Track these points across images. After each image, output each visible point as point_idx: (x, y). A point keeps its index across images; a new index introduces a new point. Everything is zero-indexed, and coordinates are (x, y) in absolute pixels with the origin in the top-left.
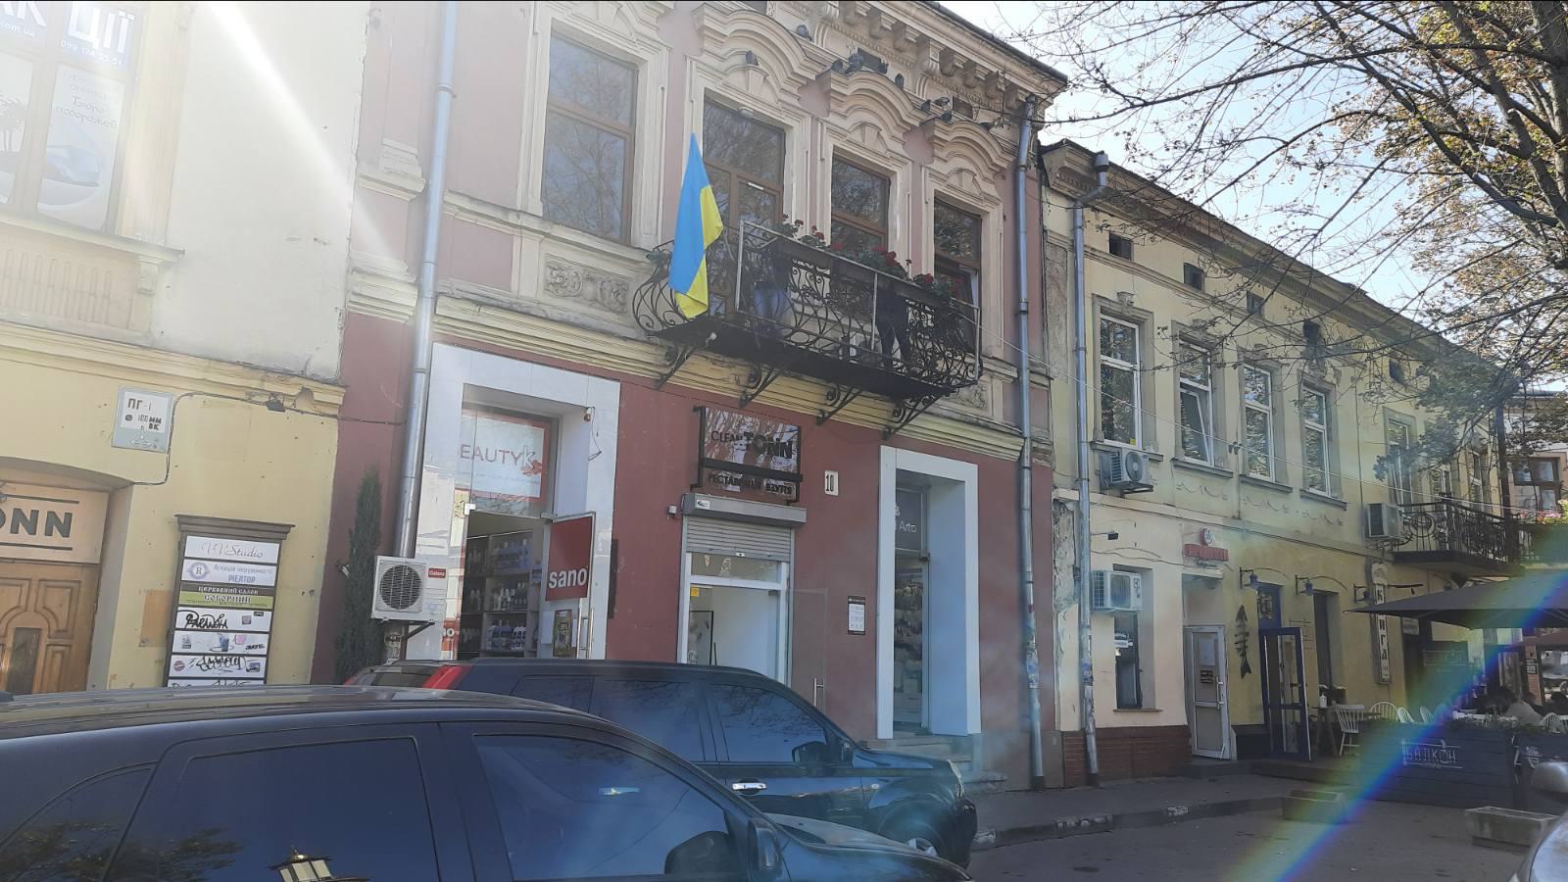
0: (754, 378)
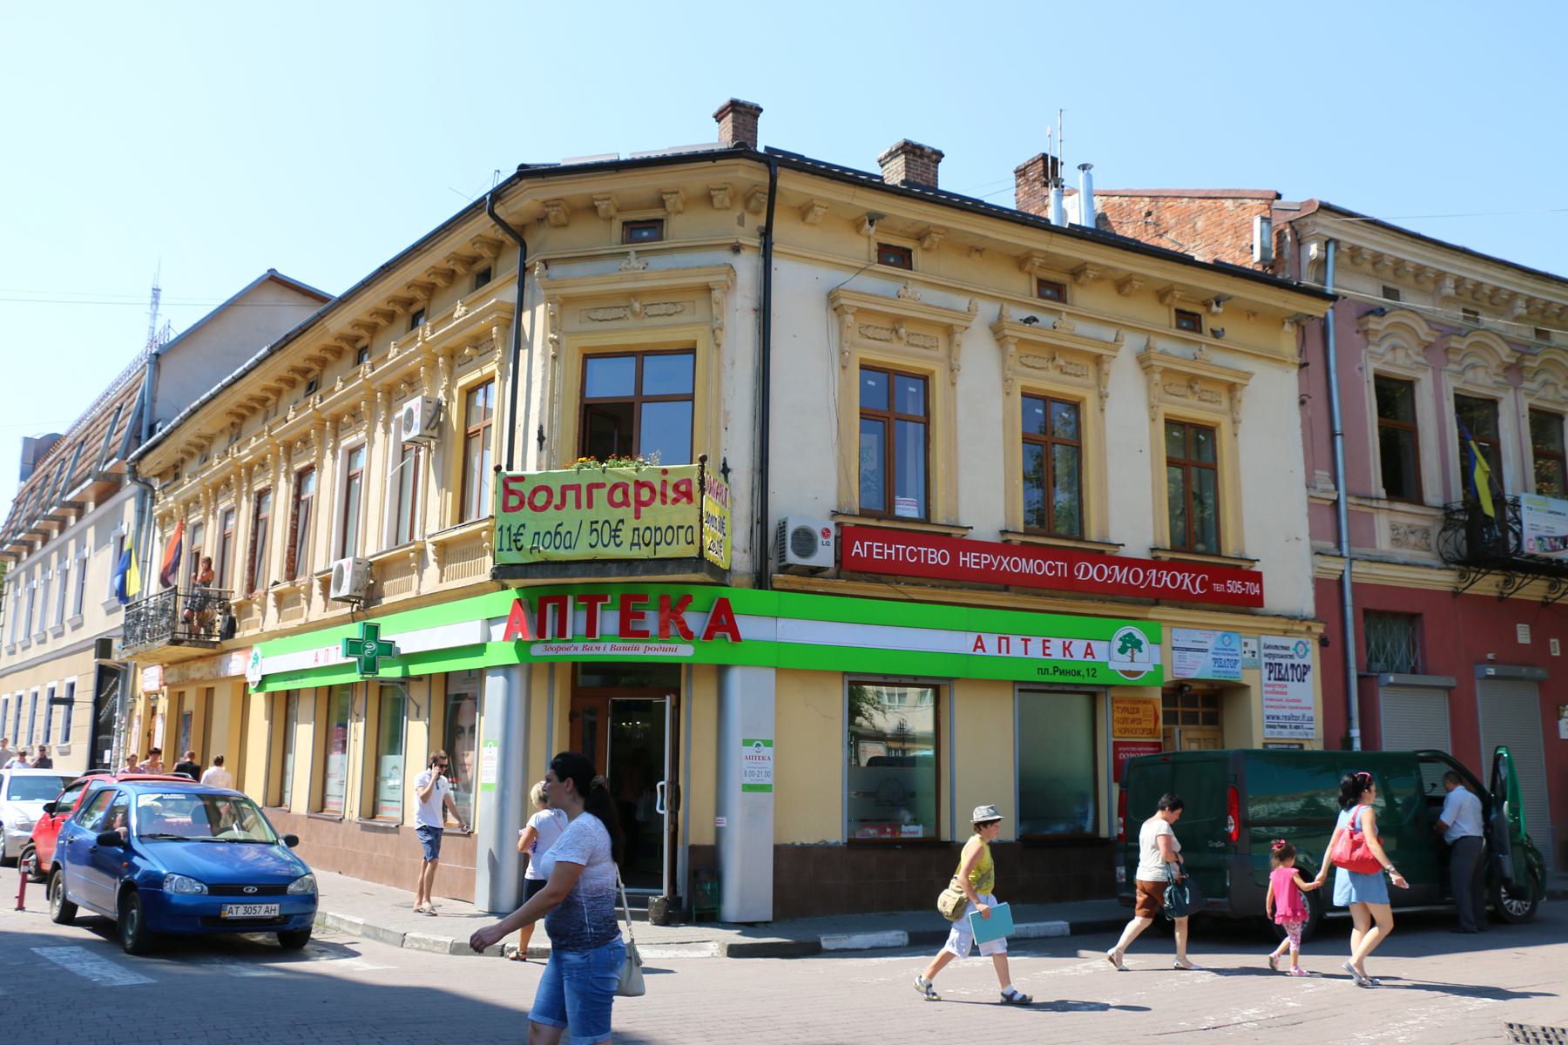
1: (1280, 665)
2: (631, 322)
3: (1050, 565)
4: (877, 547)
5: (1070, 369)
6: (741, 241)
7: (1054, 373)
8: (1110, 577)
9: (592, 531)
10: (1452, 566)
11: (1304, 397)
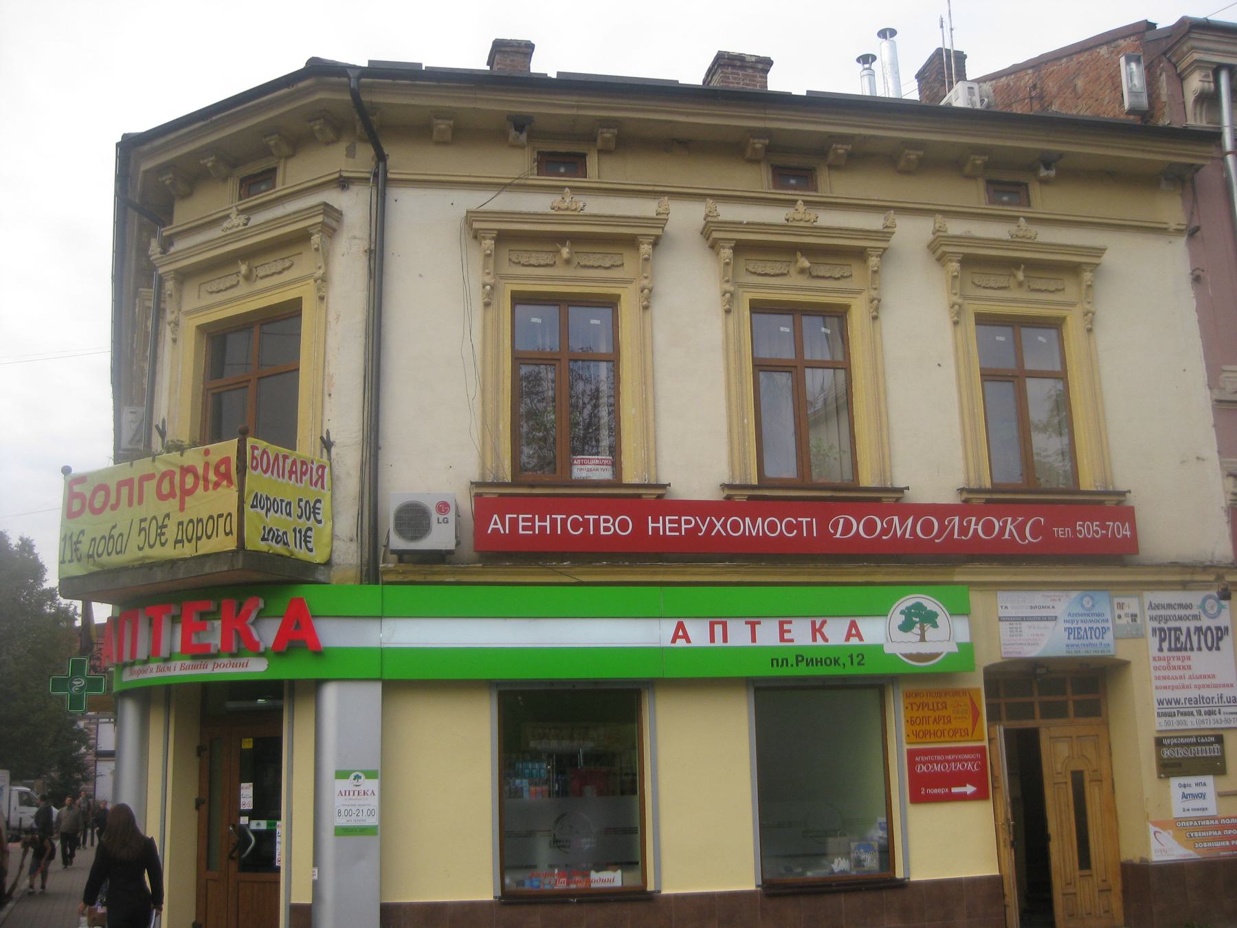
1: (1179, 629)
2: (243, 289)
3: (789, 523)
4: (524, 520)
5: (822, 271)
6: (345, 174)
7: (796, 280)
8: (885, 531)
9: (141, 531)
11: (1198, 272)
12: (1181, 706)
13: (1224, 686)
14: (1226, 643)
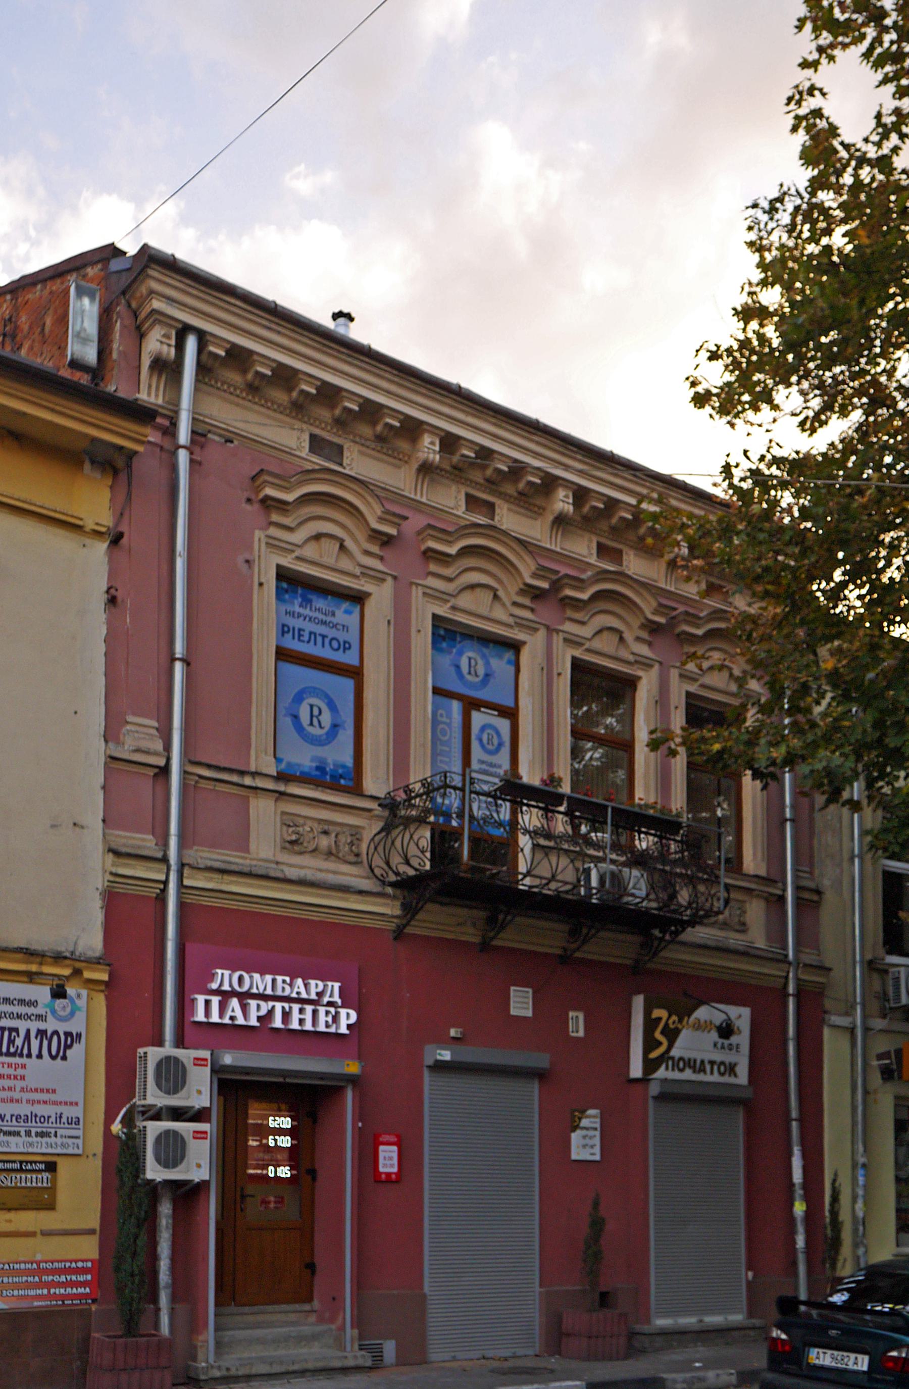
0: (491, 921)
1: (16, 1030)
10: (389, 890)
12: (5, 1123)
13: (66, 1103)
14: (76, 1052)
